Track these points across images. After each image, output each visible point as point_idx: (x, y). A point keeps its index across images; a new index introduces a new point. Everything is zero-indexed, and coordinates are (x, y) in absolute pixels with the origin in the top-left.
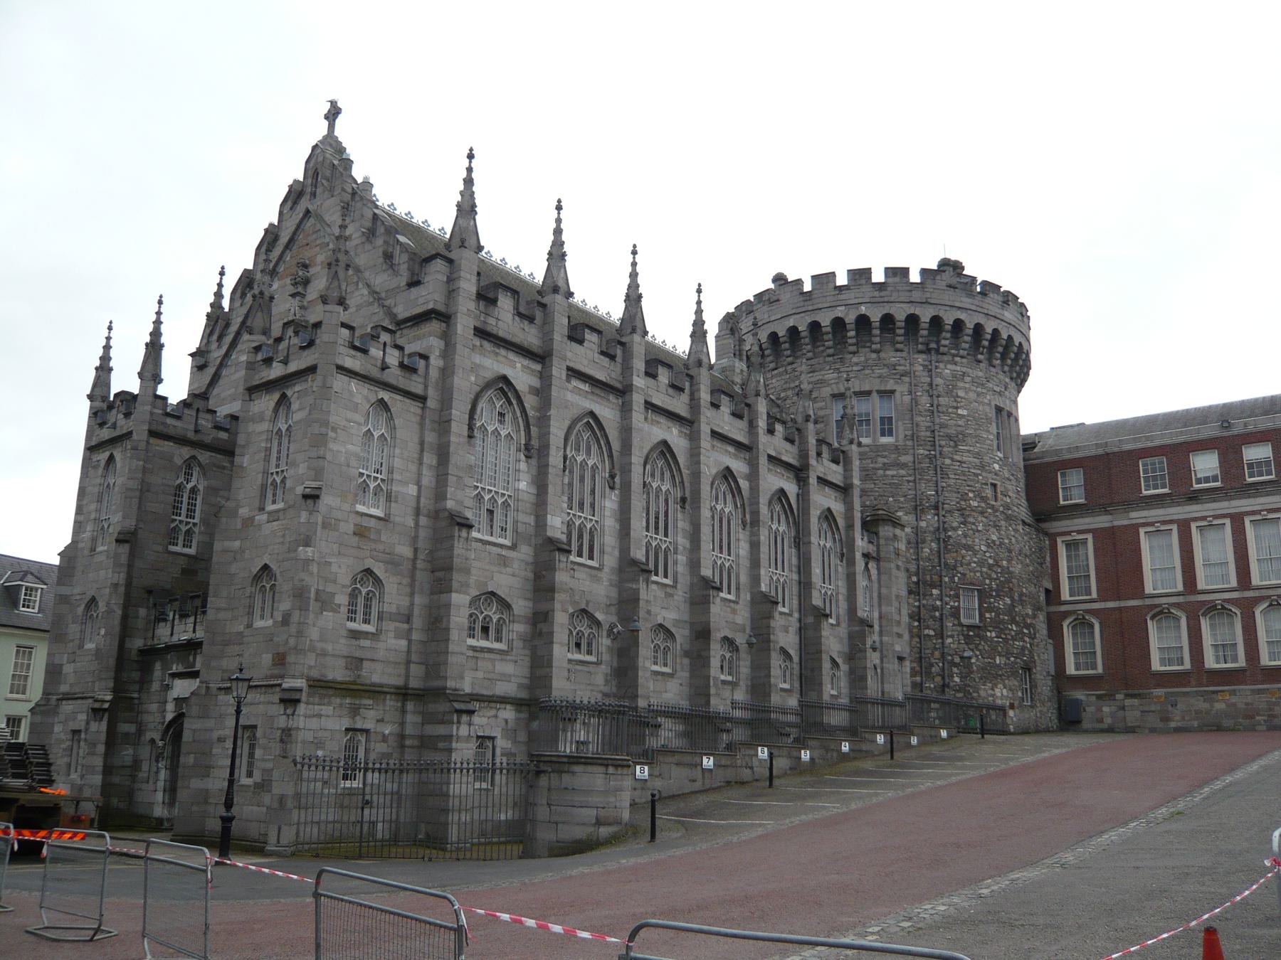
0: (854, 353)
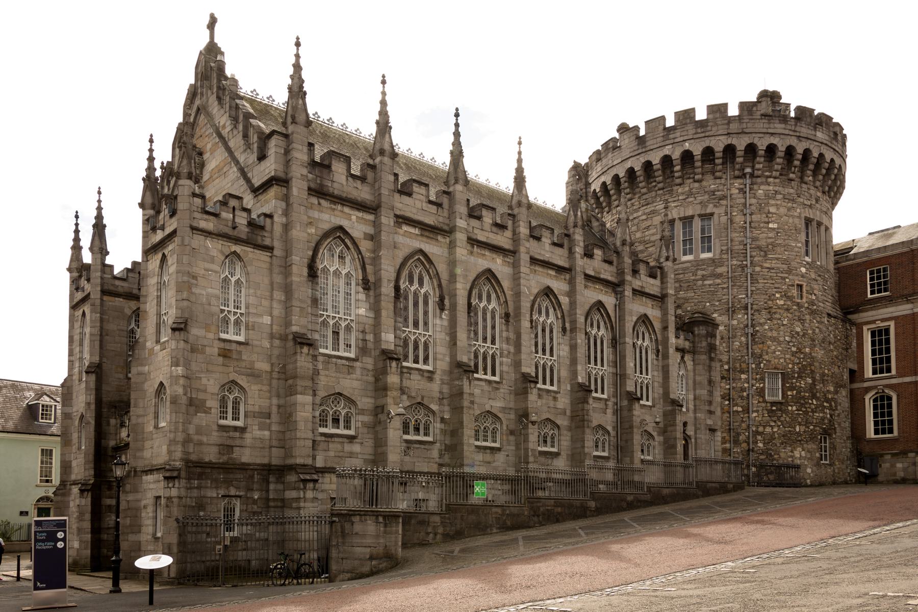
0: (680, 185)
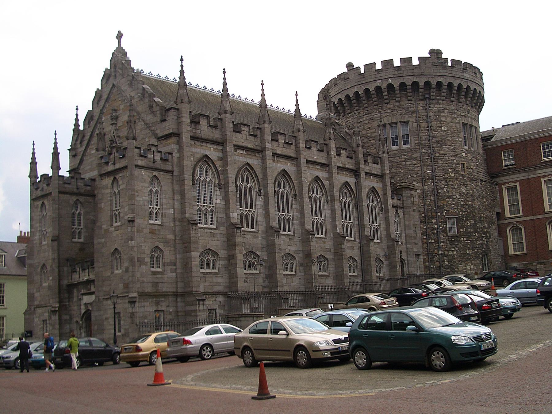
0: (388, 103)
